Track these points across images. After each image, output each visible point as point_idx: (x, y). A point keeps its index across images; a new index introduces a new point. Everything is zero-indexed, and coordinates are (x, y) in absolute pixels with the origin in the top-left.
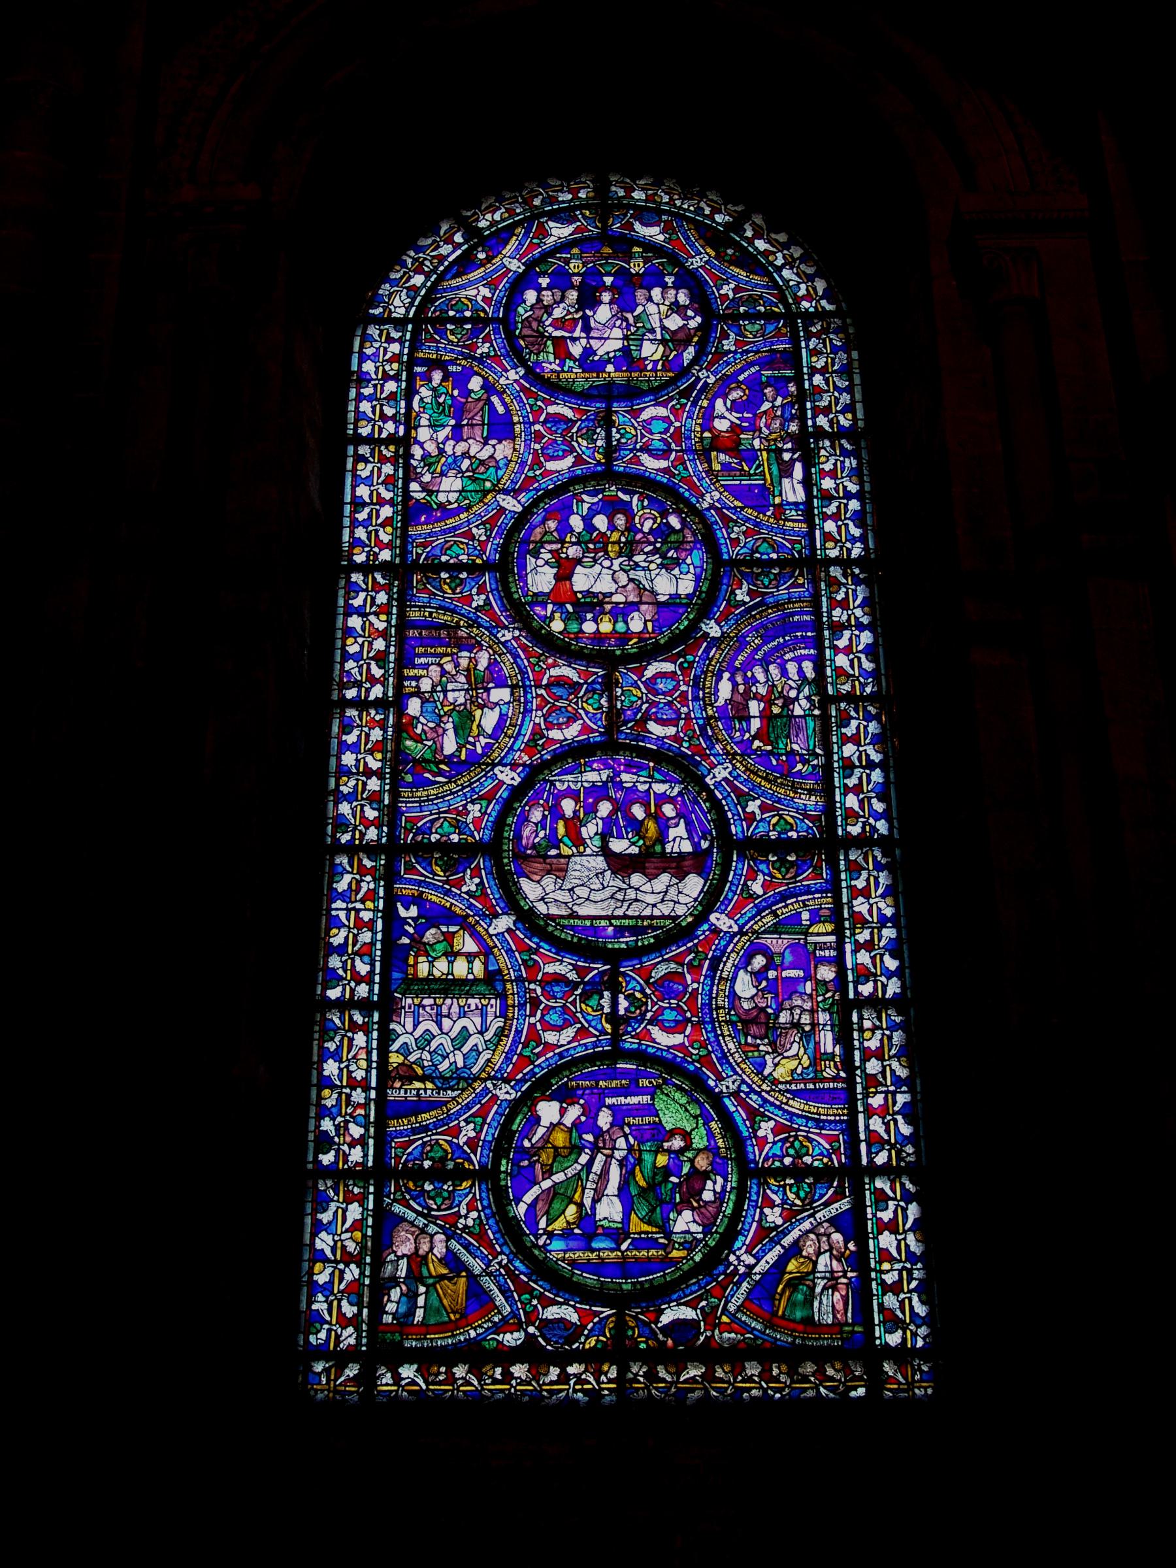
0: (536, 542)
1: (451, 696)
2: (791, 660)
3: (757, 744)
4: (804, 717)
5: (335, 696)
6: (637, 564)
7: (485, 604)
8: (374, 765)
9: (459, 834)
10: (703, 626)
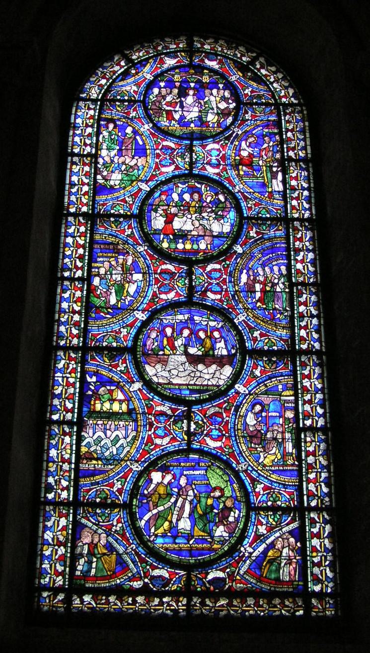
0: (156, 205)
2: (276, 265)
3: (259, 304)
4: (281, 292)
5: (59, 275)
6: (203, 217)
7: (131, 234)
8: (77, 308)
9: (117, 343)
10: (234, 248)
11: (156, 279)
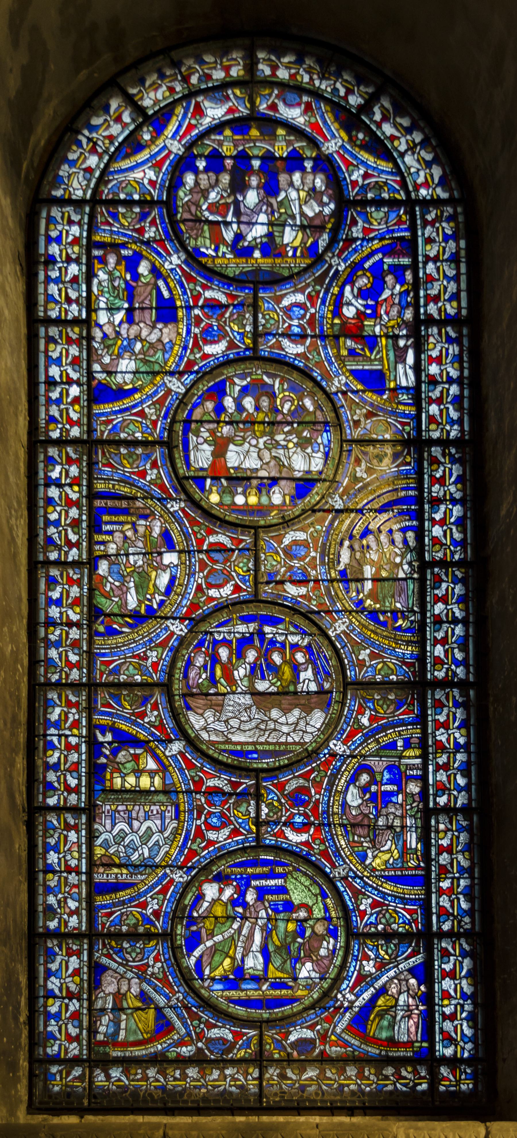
1: (131, 558)
11: (201, 561)
